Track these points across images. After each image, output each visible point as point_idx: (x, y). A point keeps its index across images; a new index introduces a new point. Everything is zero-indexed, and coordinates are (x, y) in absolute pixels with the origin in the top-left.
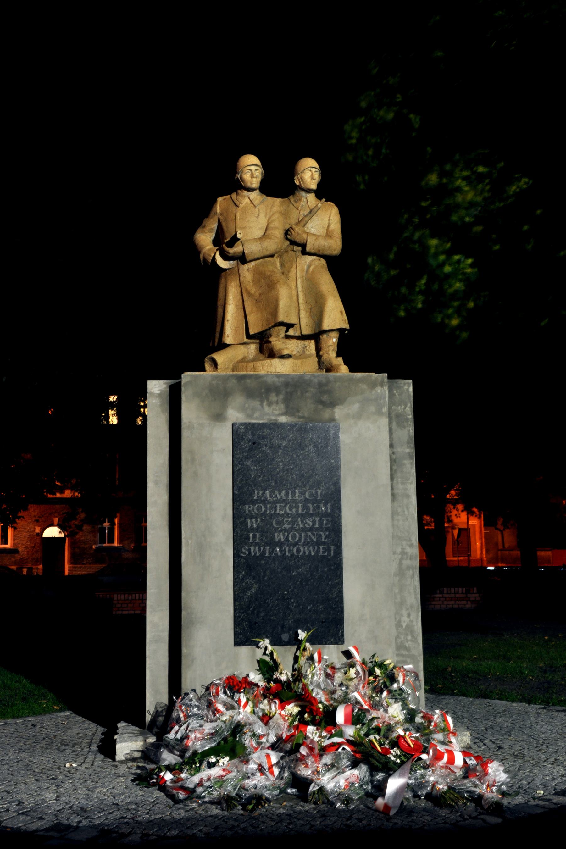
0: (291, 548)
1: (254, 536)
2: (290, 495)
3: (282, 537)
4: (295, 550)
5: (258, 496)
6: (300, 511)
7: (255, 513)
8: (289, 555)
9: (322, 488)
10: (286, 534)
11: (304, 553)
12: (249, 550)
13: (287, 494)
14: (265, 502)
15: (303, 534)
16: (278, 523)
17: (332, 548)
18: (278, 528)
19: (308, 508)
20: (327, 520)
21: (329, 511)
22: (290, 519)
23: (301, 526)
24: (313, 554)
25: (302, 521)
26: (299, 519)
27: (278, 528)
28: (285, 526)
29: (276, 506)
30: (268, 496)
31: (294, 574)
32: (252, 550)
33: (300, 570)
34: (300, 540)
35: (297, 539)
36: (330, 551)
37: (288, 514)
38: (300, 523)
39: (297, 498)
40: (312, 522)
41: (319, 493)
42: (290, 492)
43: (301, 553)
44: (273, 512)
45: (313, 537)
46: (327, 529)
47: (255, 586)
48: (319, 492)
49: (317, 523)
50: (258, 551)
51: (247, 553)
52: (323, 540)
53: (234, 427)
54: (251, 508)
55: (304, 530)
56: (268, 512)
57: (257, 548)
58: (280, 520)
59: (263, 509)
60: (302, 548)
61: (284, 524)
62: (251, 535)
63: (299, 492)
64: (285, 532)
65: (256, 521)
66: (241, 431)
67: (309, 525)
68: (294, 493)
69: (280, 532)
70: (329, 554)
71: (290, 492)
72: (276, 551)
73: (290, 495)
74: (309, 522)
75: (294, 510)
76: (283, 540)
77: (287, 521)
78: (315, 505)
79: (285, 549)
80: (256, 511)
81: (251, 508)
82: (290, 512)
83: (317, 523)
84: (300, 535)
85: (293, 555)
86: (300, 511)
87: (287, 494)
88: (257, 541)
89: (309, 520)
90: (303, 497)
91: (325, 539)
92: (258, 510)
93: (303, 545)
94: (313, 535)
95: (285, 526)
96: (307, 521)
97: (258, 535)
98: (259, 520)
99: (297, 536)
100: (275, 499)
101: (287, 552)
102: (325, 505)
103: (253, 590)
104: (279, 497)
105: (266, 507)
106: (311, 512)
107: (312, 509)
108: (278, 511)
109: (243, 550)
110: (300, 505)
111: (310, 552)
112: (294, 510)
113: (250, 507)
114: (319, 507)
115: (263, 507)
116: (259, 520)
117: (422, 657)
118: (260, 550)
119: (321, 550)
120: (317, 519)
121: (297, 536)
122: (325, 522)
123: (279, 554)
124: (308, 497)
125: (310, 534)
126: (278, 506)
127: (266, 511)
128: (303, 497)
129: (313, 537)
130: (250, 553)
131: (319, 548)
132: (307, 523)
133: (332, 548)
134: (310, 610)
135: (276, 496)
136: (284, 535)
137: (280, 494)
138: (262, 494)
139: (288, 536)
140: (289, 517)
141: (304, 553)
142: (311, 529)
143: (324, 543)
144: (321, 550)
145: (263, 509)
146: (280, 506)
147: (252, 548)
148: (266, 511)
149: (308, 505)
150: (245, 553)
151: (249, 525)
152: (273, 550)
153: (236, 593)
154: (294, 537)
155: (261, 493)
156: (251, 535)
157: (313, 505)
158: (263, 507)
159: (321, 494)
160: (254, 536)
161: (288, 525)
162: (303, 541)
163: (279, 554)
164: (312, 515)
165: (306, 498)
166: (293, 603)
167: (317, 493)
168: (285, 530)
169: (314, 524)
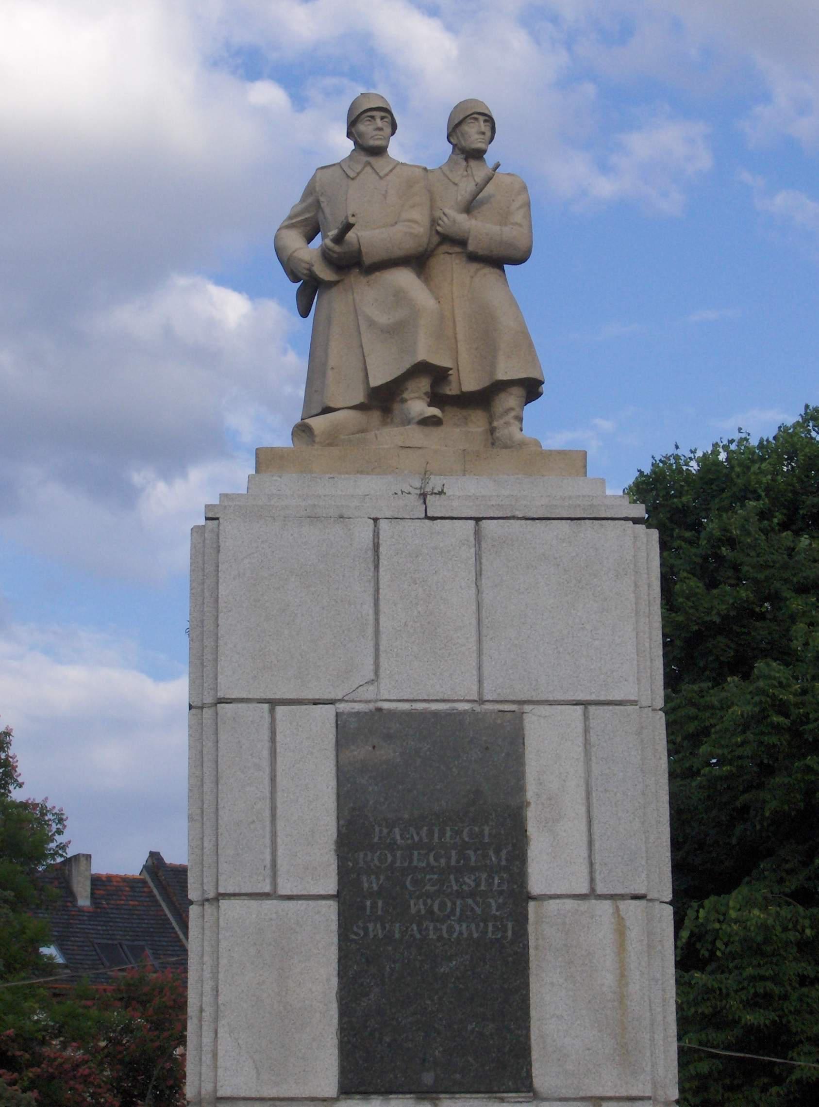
0: (438, 924)
1: (374, 906)
2: (436, 835)
3: (422, 907)
4: (444, 927)
5: (380, 838)
6: (453, 863)
7: (375, 865)
8: (435, 937)
9: (491, 823)
10: (429, 901)
11: (461, 933)
12: (366, 929)
13: (431, 833)
14: (392, 846)
15: (458, 902)
16: (415, 882)
17: (510, 925)
18: (415, 892)
19: (467, 859)
20: (501, 879)
21: (504, 863)
22: (436, 876)
23: (455, 888)
24: (475, 935)
25: (457, 881)
26: (452, 877)
27: (415, 892)
28: (428, 887)
29: (412, 854)
30: (398, 837)
31: (442, 970)
32: (371, 929)
33: (454, 963)
34: (453, 910)
35: (448, 910)
36: (506, 931)
37: (433, 867)
38: (453, 882)
39: (448, 839)
40: (475, 880)
41: (486, 832)
42: (436, 830)
43: (455, 935)
44: (406, 864)
45: (475, 907)
46: (501, 893)
47: (376, 990)
48: (487, 829)
49: (483, 883)
50: (380, 931)
51: (362, 934)
52: (494, 912)
53: (339, 719)
54: (369, 858)
55: (460, 894)
56: (398, 864)
57: (378, 926)
58: (419, 877)
59: (390, 859)
60: (457, 927)
61: (425, 886)
62: (368, 903)
63: (451, 829)
64: (428, 897)
65: (378, 879)
66: (352, 727)
67: (470, 886)
68: (442, 834)
69: (418, 898)
70: (504, 937)
71: (436, 830)
72: (412, 930)
73: (436, 835)
74: (469, 880)
75: (443, 861)
76: (423, 912)
77: (430, 879)
78: (479, 852)
79: (427, 929)
80: (376, 862)
81: (369, 858)
82: (436, 864)
83: (483, 883)
84: (454, 904)
85: (440, 938)
86: (453, 863)
87: (431, 833)
88: (379, 913)
89: (469, 878)
90: (458, 839)
91: (497, 910)
92: (380, 859)
93: (460, 921)
94: (477, 903)
95: (428, 887)
96: (467, 880)
97: (380, 904)
98: (382, 877)
99: (449, 904)
100: (409, 842)
101: (431, 933)
102: (498, 852)
103: (372, 996)
104: (416, 838)
105: (394, 856)
106: (473, 864)
107: (473, 859)
108: (415, 863)
109: (355, 929)
110: (453, 853)
111: (471, 934)
112: (443, 861)
113: (366, 855)
114: (485, 856)
115: (389, 855)
116: (382, 877)
117: (531, 959)
118: (383, 928)
119: (490, 929)
120: (484, 876)
121: (449, 904)
122: (496, 881)
123: (418, 936)
124: (467, 839)
125: (470, 901)
126: (416, 853)
127: (393, 862)
128: (458, 839)
129: (475, 907)
130: (366, 933)
131: (486, 926)
132: (465, 883)
133: (510, 925)
134: (473, 1031)
135: (412, 836)
136: (425, 904)
137: (418, 834)
138: (388, 834)
139: (432, 905)
140: (434, 873)
141: (461, 933)
142: (472, 894)
143: (495, 917)
144: (490, 929)
145: (390, 859)
146: (419, 854)
147: (371, 926)
148: (393, 862)
149: (468, 852)
150: (356, 934)
151: (366, 885)
152: (407, 928)
153: (344, 1002)
154: (442, 906)
155: (385, 831)
156: (368, 903)
157: (475, 851)
158: (389, 855)
159: (490, 834)
160: (374, 906)
161: (433, 886)
162: (458, 913)
163: (418, 936)
164: (473, 870)
165: (463, 841)
166: (441, 1019)
167: (482, 832)
168: (429, 895)
169: (478, 885)
